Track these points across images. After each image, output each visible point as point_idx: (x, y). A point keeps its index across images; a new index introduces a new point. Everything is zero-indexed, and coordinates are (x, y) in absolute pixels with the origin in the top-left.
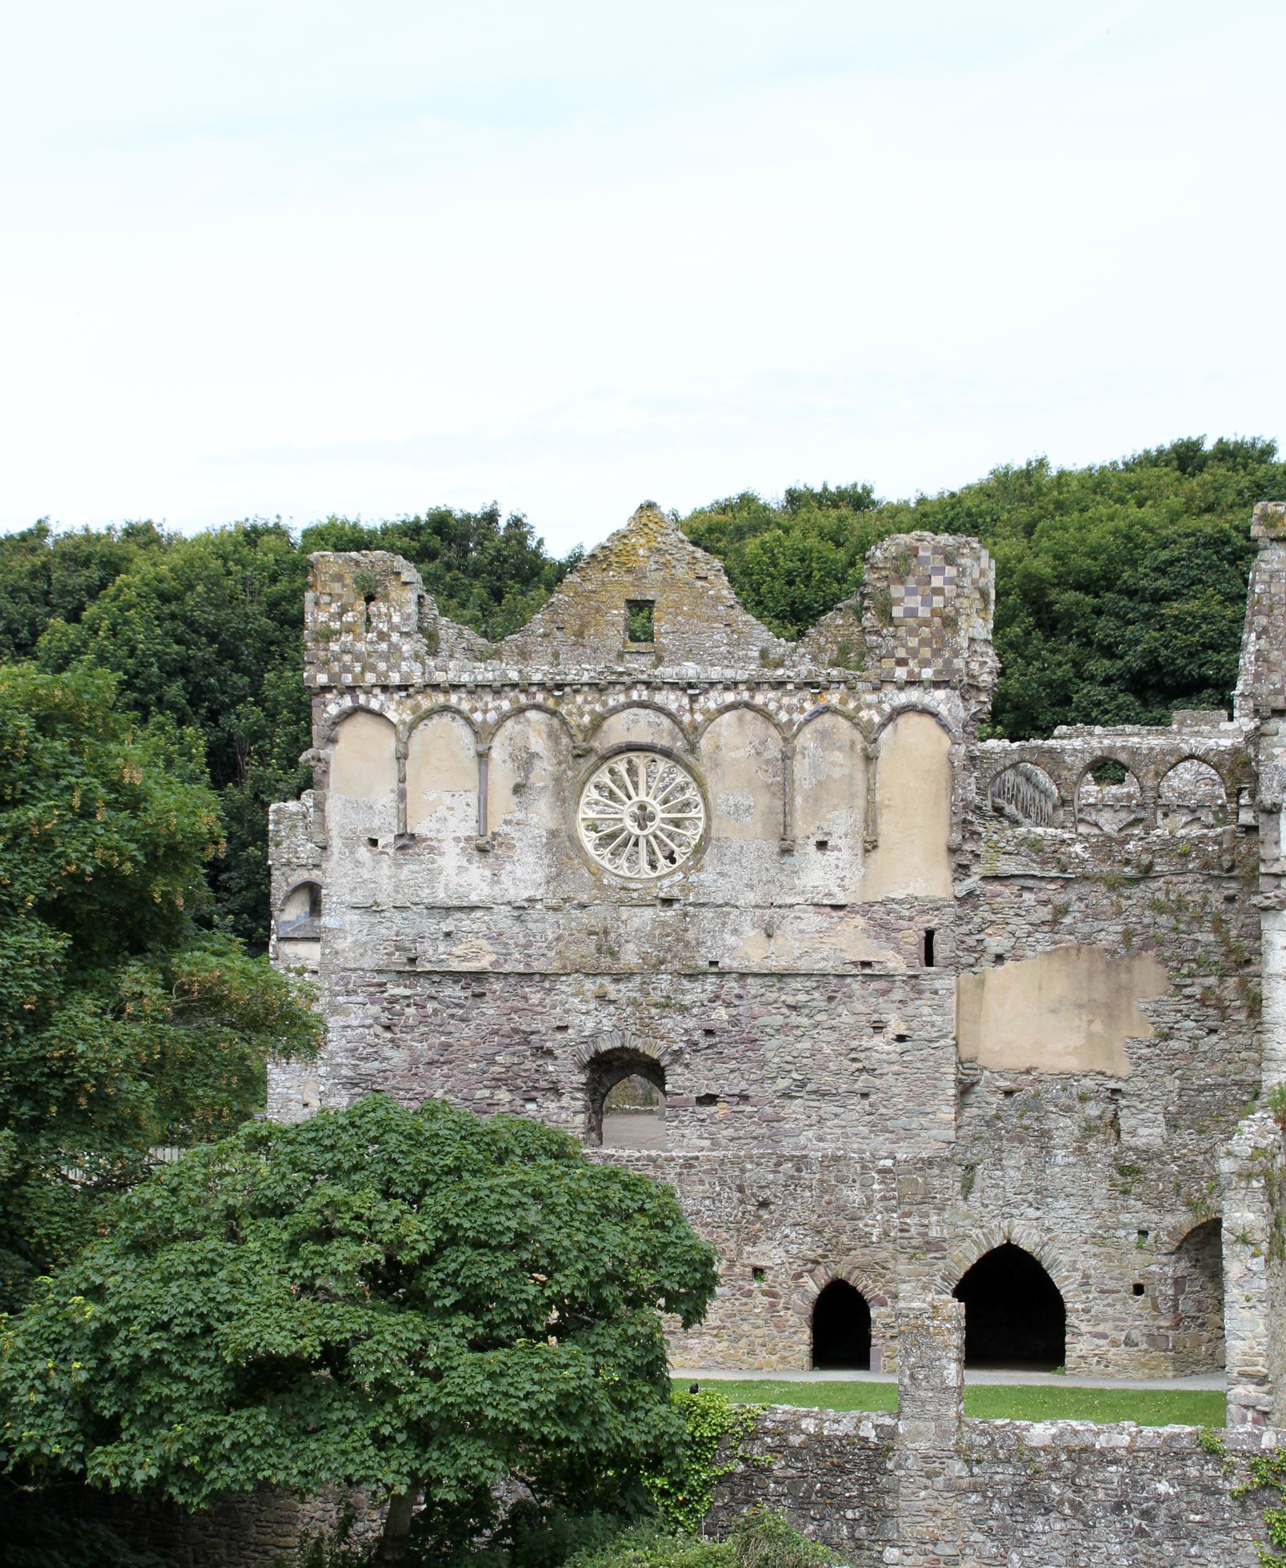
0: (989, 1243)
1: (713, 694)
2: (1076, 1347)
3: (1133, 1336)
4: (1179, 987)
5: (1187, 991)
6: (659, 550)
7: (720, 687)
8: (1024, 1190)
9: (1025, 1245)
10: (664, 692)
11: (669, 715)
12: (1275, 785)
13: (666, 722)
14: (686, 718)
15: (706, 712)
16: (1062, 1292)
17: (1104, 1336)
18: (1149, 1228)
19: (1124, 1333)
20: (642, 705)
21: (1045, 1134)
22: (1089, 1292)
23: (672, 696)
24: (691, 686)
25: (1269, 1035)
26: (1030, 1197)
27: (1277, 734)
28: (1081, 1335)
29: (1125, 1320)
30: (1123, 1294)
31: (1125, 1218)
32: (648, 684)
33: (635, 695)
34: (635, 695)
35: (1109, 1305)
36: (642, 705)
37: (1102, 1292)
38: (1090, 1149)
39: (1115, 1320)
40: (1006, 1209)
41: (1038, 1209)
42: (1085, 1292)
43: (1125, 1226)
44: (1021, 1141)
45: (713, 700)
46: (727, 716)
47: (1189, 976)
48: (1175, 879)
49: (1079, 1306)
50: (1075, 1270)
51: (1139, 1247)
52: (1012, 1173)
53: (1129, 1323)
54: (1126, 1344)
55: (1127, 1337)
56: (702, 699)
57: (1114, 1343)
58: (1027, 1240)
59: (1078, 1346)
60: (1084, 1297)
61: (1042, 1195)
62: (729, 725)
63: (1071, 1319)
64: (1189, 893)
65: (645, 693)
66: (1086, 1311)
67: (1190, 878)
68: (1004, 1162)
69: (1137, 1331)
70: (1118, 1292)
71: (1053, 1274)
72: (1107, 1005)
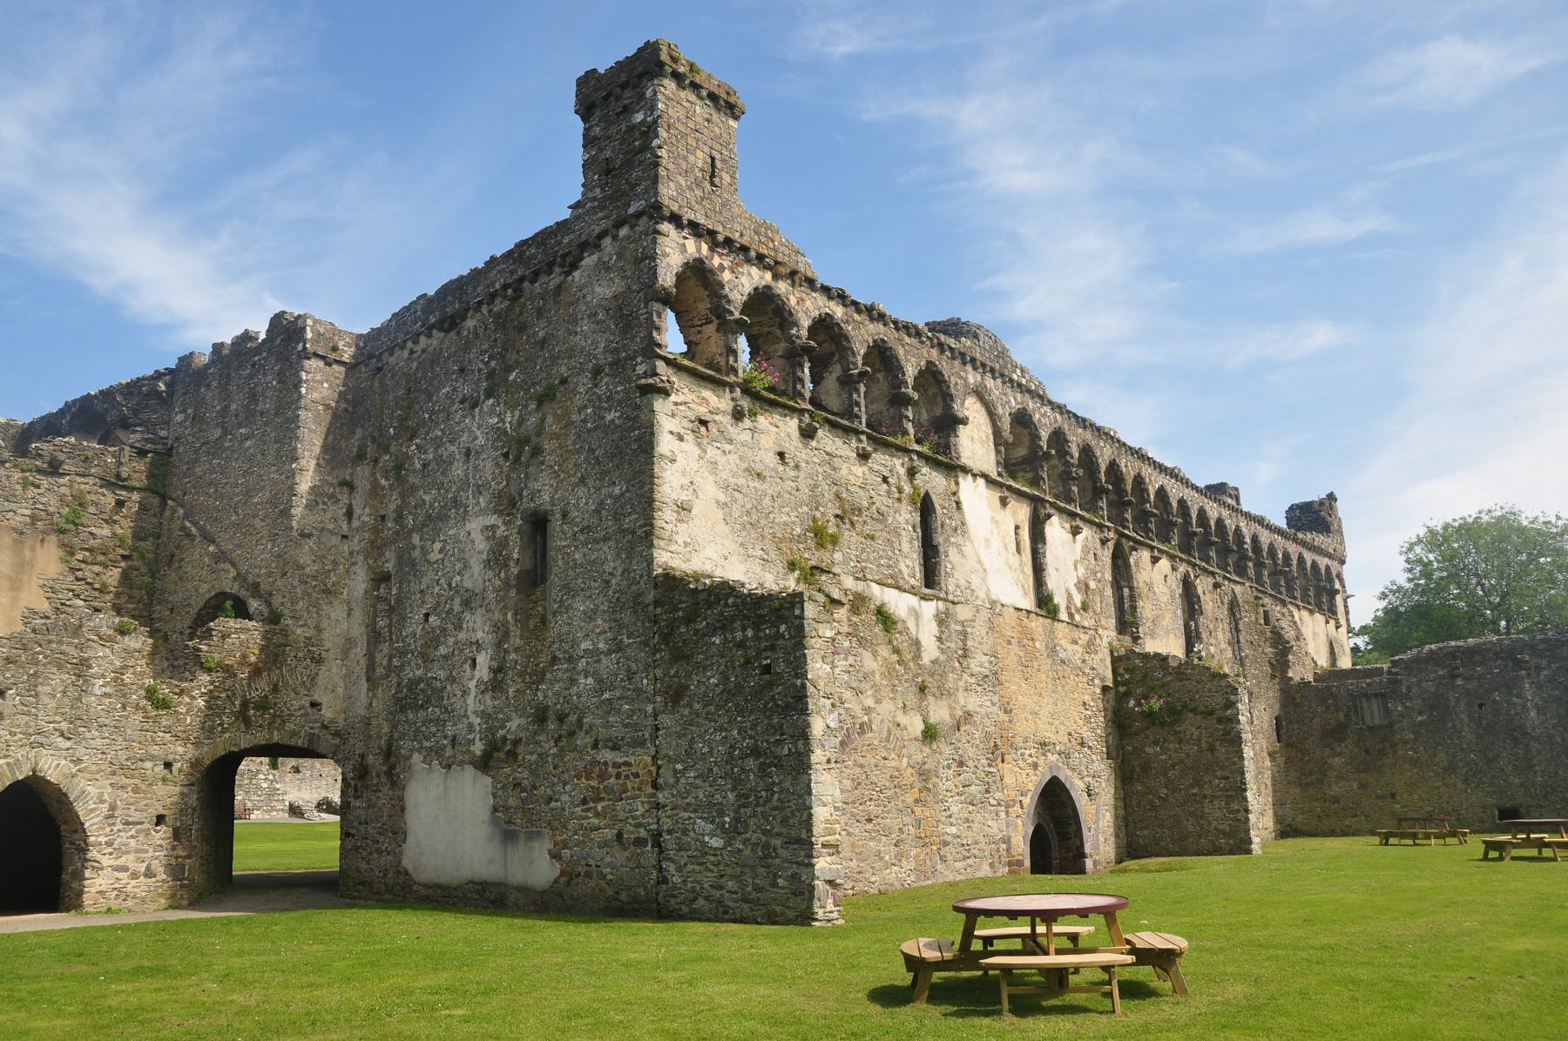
0: (13, 773)
2: (97, 884)
3: (153, 867)
4: (73, 570)
5: (80, 574)
8: (57, 718)
9: (53, 777)
16: (86, 826)
17: (124, 869)
18: (175, 760)
19: (145, 865)
21: (85, 663)
22: (114, 824)
25: (660, 513)
26: (64, 726)
28: (102, 869)
29: (146, 851)
30: (146, 826)
31: (154, 750)
35: (132, 837)
37: (127, 823)
38: (128, 681)
39: (137, 851)
40: (40, 739)
41: (69, 739)
42: (109, 825)
43: (152, 758)
44: (59, 667)
47: (83, 561)
48: (79, 479)
49: (103, 839)
50: (102, 801)
51: (164, 780)
52: (46, 700)
53: (150, 854)
54: (146, 875)
55: (148, 868)
57: (135, 876)
58: (53, 768)
59: (98, 881)
60: (108, 829)
61: (76, 724)
63: (93, 853)
64: (89, 492)
66: (110, 844)
67: (91, 481)
68: (40, 688)
69: (157, 862)
70: (142, 823)
71: (80, 809)
72: (9, 577)
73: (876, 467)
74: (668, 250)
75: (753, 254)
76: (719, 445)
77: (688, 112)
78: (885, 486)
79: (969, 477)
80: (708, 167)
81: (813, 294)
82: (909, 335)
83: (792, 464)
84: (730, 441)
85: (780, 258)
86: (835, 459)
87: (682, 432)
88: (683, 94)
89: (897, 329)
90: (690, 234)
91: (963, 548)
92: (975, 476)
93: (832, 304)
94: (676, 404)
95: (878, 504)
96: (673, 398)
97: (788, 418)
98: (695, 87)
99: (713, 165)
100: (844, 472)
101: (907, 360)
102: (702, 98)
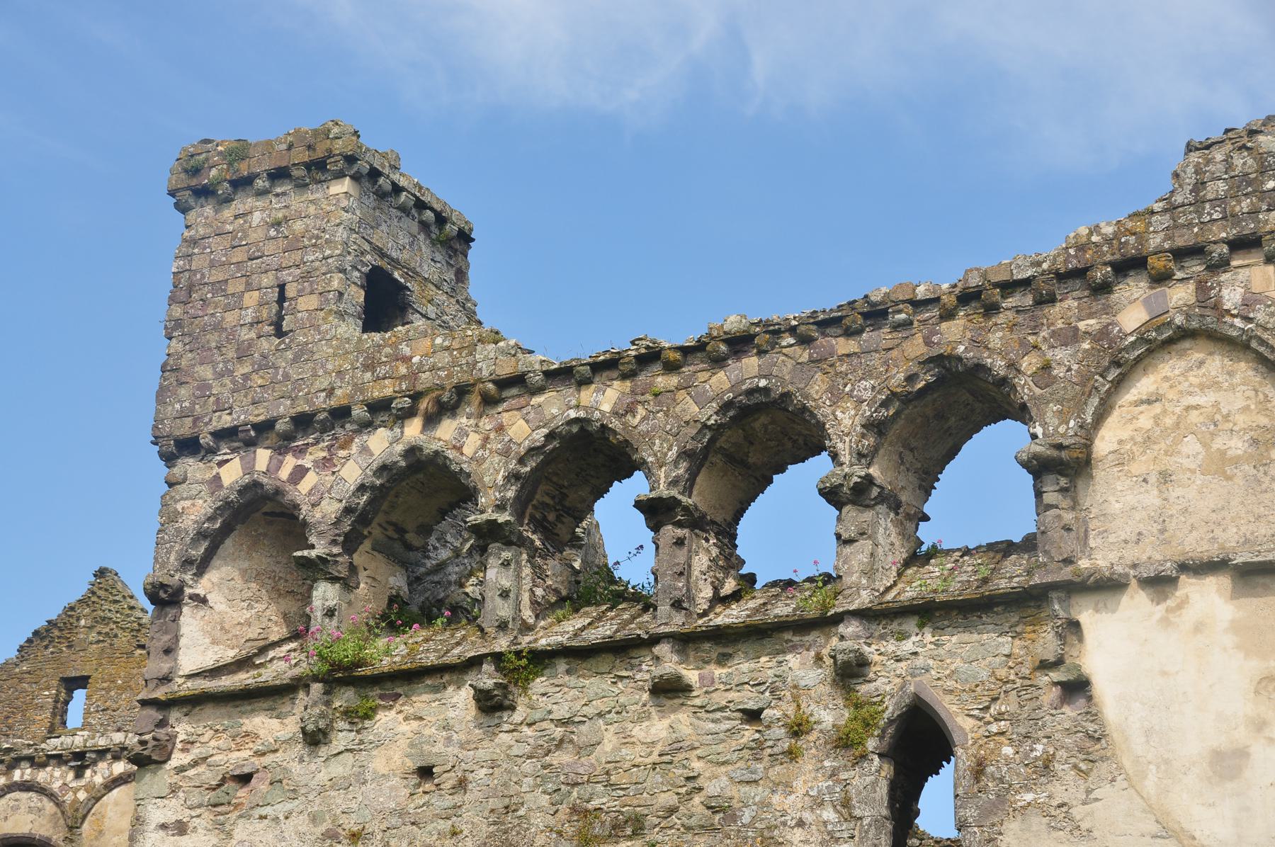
1: (102, 765)
6: (104, 619)
7: (109, 756)
10: (49, 769)
11: (51, 796)
12: (172, 558)
13: (49, 806)
14: (69, 797)
15: (89, 788)
20: (26, 787)
23: (57, 773)
24: (80, 756)
27: (184, 482)
32: (31, 759)
33: (17, 775)
34: (17, 775)
36: (26, 787)
45: (99, 774)
46: (115, 791)
56: (88, 773)
62: (116, 804)
65: (29, 771)
73: (720, 699)
74: (179, 507)
75: (358, 412)
76: (263, 811)
77: (233, 239)
78: (749, 733)
79: (1136, 602)
80: (269, 312)
81: (536, 400)
82: (850, 333)
83: (449, 781)
84: (294, 793)
85: (426, 379)
86: (583, 728)
87: (184, 815)
88: (228, 213)
89: (805, 341)
90: (234, 450)
91: (1078, 812)
92: (1159, 584)
93: (588, 396)
94: (181, 770)
95: (712, 788)
96: (178, 759)
97: (450, 689)
98: (242, 183)
99: (282, 298)
100: (609, 742)
101: (837, 396)
102: (262, 193)
